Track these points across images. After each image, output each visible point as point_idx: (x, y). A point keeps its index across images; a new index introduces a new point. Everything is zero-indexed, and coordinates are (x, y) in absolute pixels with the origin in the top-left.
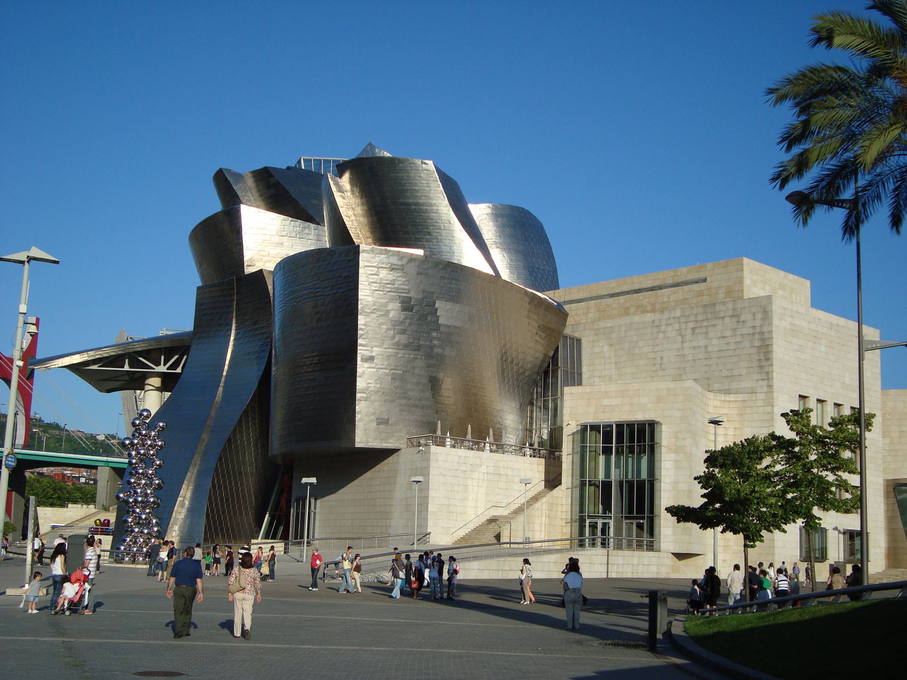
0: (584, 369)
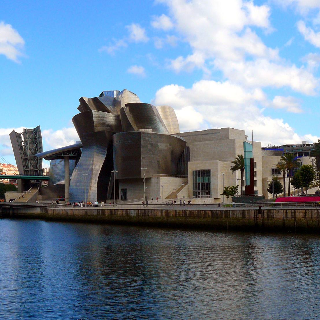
0: (190, 154)
